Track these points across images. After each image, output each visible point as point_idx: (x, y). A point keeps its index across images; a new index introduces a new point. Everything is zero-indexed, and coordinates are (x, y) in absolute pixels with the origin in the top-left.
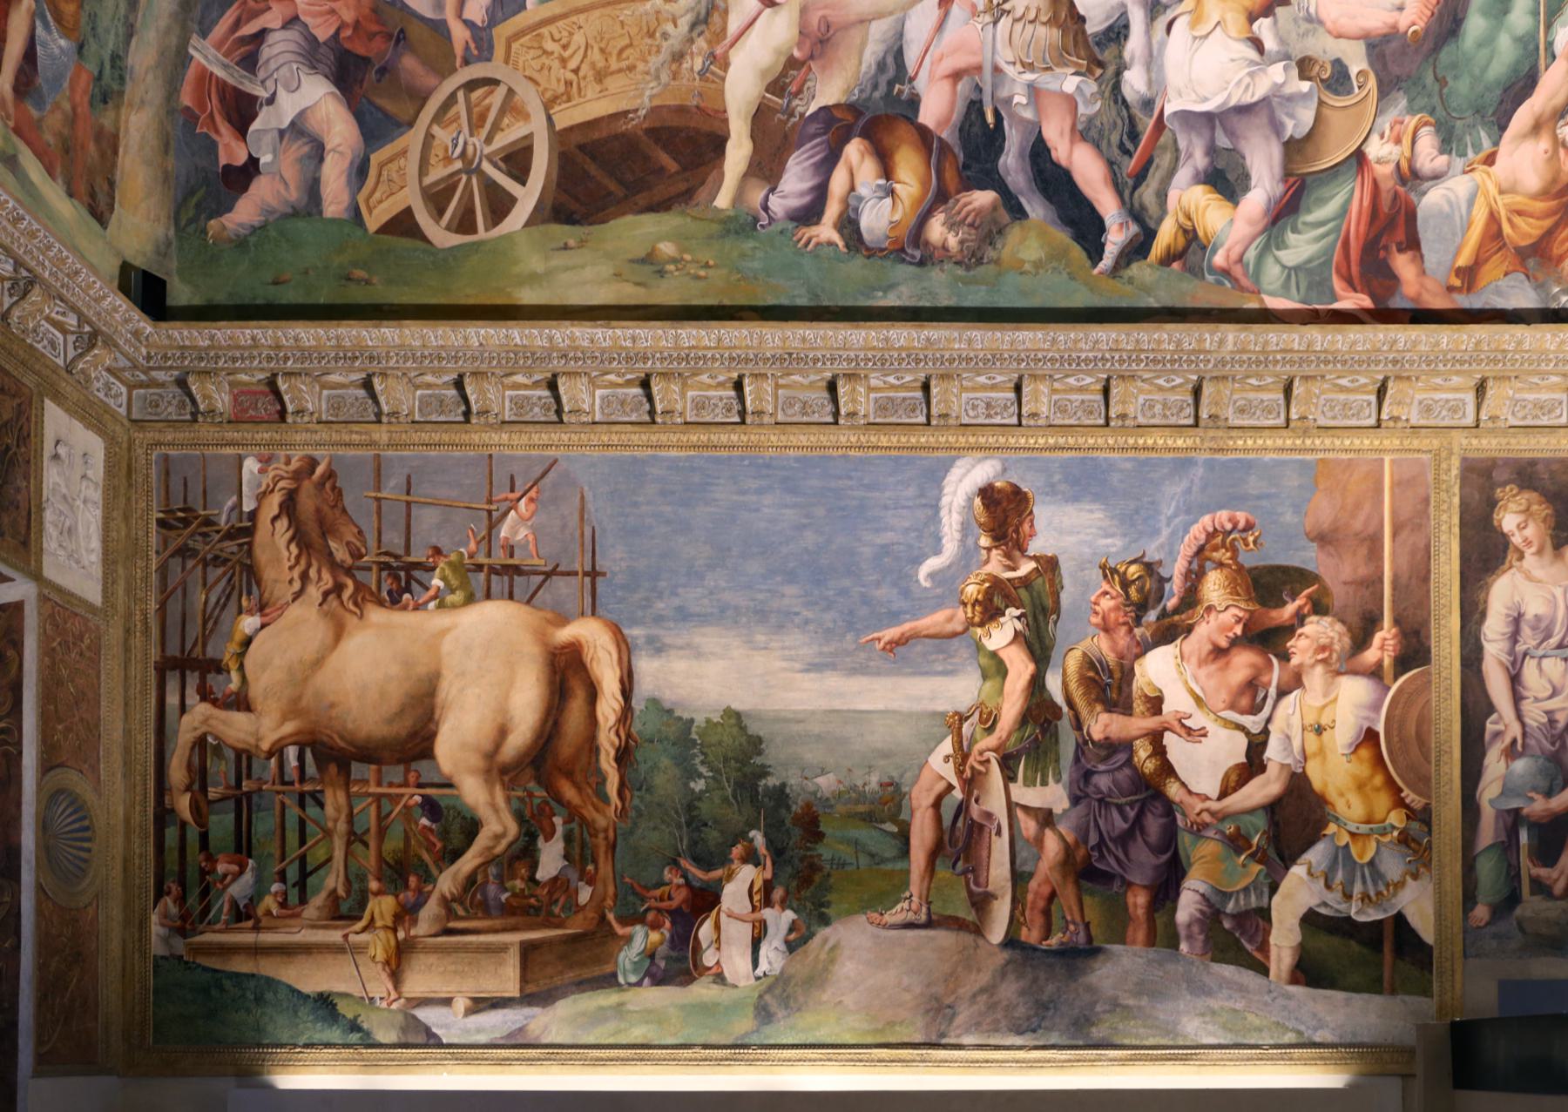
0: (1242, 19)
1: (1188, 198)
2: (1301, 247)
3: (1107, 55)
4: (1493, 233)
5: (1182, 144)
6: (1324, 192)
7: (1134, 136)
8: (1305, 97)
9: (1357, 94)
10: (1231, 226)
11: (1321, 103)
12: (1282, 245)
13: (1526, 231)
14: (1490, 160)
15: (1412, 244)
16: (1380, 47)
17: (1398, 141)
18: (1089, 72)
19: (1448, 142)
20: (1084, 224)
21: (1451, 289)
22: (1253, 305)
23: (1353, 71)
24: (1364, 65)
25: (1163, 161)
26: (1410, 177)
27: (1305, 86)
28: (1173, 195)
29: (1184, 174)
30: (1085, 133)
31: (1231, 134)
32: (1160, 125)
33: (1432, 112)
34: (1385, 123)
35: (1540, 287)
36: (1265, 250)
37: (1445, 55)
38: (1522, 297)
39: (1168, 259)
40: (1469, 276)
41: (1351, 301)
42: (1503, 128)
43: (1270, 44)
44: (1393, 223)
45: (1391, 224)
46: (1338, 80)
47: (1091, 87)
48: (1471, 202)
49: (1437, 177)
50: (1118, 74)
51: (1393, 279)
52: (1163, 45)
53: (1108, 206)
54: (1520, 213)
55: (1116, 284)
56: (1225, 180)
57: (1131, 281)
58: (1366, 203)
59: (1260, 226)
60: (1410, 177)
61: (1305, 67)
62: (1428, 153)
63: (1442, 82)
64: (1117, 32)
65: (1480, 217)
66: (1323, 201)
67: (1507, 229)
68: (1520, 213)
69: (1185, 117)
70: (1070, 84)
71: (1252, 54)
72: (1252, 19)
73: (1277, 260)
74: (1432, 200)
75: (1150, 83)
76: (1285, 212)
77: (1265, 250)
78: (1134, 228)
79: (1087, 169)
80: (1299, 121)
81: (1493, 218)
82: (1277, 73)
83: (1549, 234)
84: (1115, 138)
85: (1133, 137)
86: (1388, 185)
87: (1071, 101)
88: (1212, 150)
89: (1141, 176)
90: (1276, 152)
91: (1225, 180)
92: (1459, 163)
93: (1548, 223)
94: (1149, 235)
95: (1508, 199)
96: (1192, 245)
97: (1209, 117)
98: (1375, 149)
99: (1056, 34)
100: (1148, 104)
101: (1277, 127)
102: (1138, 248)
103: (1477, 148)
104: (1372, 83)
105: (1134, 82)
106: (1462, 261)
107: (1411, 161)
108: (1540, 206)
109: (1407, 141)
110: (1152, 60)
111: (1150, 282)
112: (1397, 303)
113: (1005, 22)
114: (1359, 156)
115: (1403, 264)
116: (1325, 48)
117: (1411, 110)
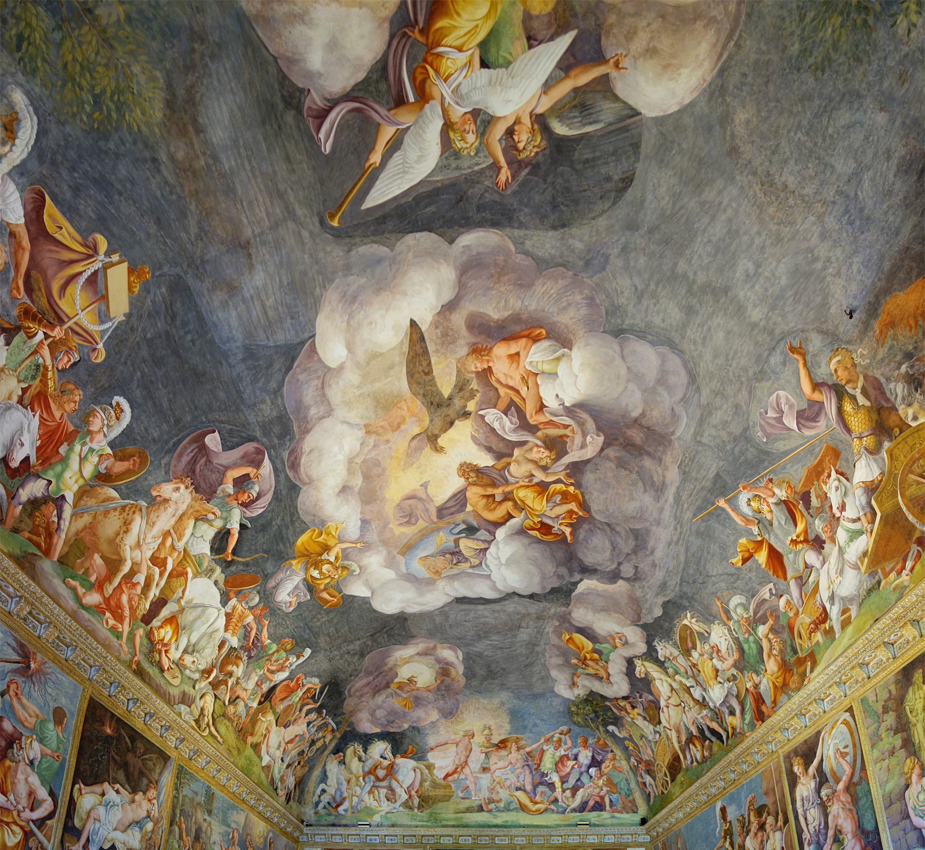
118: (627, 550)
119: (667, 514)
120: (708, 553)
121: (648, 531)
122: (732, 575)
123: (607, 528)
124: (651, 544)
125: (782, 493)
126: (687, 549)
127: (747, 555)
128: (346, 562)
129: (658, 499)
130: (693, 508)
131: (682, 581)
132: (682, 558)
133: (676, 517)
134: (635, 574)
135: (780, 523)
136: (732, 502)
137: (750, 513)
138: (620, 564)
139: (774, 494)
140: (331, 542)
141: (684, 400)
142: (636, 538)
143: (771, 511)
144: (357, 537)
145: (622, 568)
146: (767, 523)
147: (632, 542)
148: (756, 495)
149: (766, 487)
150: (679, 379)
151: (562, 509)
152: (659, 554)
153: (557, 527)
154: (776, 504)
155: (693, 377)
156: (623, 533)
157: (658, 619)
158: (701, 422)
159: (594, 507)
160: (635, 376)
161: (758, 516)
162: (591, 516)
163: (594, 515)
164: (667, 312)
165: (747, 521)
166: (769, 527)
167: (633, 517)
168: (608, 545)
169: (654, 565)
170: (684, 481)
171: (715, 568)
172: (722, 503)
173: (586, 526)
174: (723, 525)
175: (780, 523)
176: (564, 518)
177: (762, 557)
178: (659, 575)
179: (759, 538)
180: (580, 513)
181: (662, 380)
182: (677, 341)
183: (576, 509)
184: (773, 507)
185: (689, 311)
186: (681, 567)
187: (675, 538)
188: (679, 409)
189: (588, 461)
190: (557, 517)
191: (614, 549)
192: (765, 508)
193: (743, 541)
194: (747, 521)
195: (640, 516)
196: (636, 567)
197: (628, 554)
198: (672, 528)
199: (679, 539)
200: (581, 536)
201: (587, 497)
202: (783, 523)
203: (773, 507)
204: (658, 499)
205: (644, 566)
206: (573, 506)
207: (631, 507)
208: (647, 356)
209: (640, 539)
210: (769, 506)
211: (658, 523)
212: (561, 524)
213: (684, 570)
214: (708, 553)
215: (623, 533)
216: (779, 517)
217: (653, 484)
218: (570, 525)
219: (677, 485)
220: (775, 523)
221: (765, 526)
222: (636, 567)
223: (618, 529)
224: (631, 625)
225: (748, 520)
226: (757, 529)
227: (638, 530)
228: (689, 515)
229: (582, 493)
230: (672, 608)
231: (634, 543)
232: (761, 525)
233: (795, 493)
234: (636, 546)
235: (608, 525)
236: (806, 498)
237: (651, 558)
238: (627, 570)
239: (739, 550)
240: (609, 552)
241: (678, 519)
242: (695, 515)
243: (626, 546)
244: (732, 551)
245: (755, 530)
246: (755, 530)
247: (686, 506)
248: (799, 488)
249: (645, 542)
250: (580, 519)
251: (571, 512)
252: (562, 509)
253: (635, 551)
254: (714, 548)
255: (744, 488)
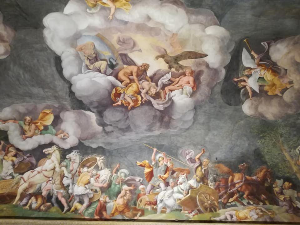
0: (84, 185)
1: (76, 204)
2: (90, 210)
3: (67, 188)
4: (116, 209)
5: (76, 198)
6: (94, 204)
7: (70, 197)
8: (92, 193)
9: (98, 193)
10: (81, 208)
11: (94, 194)
12: (88, 210)
13: (121, 209)
14: (116, 201)
15: (105, 210)
16: (101, 188)
17: (104, 198)
18: (64, 190)
19: (110, 198)
20: (61, 207)
21: (110, 216)
22: (83, 218)
23: (98, 190)
24: (99, 190)
25: (73, 200)
26: (106, 202)
27: (92, 192)
28: (74, 204)
29: (76, 202)
30: (63, 197)
31: (82, 197)
32: (73, 196)
33: (108, 195)
34: (102, 196)
35: (122, 216)
36: (86, 210)
37: (110, 189)
38: (120, 217)
39: (72, 212)
40: (113, 214)
41: (96, 217)
42: (117, 197)
43: (87, 188)
44: (103, 208)
45: (103, 208)
46: (96, 191)
47: (65, 192)
48: (113, 205)
49: (109, 202)
50: (68, 190)
51: (103, 215)
52: (74, 187)
53: (65, 205)
54: (120, 207)
55: (65, 214)
56: (81, 202)
57: (67, 214)
58: (100, 205)
59: (85, 208)
60: (106, 202)
61: (92, 190)
62: (108, 199)
63: (109, 192)
64: (68, 186)
65: (115, 207)
66: (94, 205)
67: (118, 209)
68: (120, 207)
69: (77, 195)
70: (62, 191)
71: (85, 188)
72: (85, 185)
73: (87, 212)
74: (108, 205)
75: (72, 191)
76: (89, 206)
77: (86, 210)
78: (68, 208)
79: (63, 201)
80: (91, 196)
81: (116, 207)
82: (88, 191)
83: (124, 209)
84: (67, 197)
85: (70, 198)
86: (103, 203)
87: (62, 193)
88: (80, 199)
89: (70, 202)
90: (88, 199)
91: (81, 202)
92: (112, 201)
93: (123, 208)
94: (70, 209)
95: (119, 205)
96: (76, 210)
97: (79, 195)
98: (101, 199)
99: (60, 186)
100: (72, 194)
101: (88, 196)
102: (69, 210)
103: (114, 199)
104: (100, 192)
105: (70, 191)
106: (112, 213)
107: (106, 200)
108: (122, 206)
109: (105, 198)
110: (72, 189)
111: (69, 215)
112: (103, 218)
113: (54, 185)
114: (99, 200)
115: (104, 213)
116: (94, 188)
117: (105, 195)
118: (119, 126)
119: (142, 135)
120: (135, 153)
121: (131, 131)
122: (132, 164)
123: (126, 117)
124: (126, 133)
125: (169, 165)
126: (131, 146)
127: (143, 165)
128: (99, 8)
129: (146, 130)
130: (148, 142)
131: (117, 149)
132: (127, 146)
133: (142, 138)
134: (109, 132)
135: (161, 169)
136: (157, 153)
137: (157, 159)
138: (111, 125)
139: (167, 163)
140: (118, 4)
141: (181, 129)
142: (126, 128)
143: (162, 165)
144: (118, 18)
145: (109, 126)
146: (158, 165)
147: (124, 127)
148: (163, 158)
149: (168, 160)
150: (187, 126)
151: (129, 100)
152: (124, 137)
153: (120, 99)
154: (165, 165)
155: (188, 129)
156: (126, 123)
157: (89, 147)
158: (177, 135)
159: (134, 111)
160: (184, 115)
161: (158, 162)
162: (129, 111)
163: (130, 112)
164: (202, 119)
165: (154, 160)
166: (157, 167)
167: (135, 125)
168: (117, 119)
169: (118, 138)
170: (156, 136)
171: (130, 158)
172: (155, 150)
173: (124, 110)
174: (148, 153)
175: (161, 169)
176: (125, 101)
177: (147, 170)
178: (114, 141)
179: (152, 166)
180: (129, 107)
181: (185, 122)
182: (196, 123)
183: (131, 105)
184: (163, 164)
185: (203, 124)
186: (123, 147)
187: (134, 141)
188: (178, 129)
189: (153, 106)
190: (125, 99)
191: (117, 121)
192: (162, 162)
193: (147, 162)
194: (154, 160)
195: (136, 127)
196: (113, 132)
197: (117, 127)
198: (137, 138)
199: (134, 142)
200: (118, 109)
201: (138, 108)
202: (162, 170)
203: (163, 164)
204: (146, 130)
205: (115, 134)
206: (132, 104)
207: (138, 123)
208: (190, 117)
209: (128, 129)
210: (163, 163)
211: (137, 133)
212: (122, 101)
213: (123, 148)
214: (135, 153)
215: (126, 123)
216: (162, 168)
217: (152, 128)
218: (122, 104)
219: (155, 135)
220: (160, 168)
221: (156, 165)
222: (113, 132)
223: (128, 121)
224: (78, 138)
225: (155, 159)
226: (154, 163)
227: (130, 128)
228: (145, 142)
229: (139, 106)
230: (100, 151)
231: (124, 128)
232: (156, 164)
233: (172, 168)
234: (123, 129)
235: (128, 117)
236: (173, 172)
237: (119, 135)
238: (109, 129)
239: (143, 162)
240: (115, 120)
241: (142, 139)
242: (146, 144)
243: (121, 125)
244: (141, 160)
245: (153, 163)
246: (153, 163)
247: (148, 140)
248: (174, 169)
249: (126, 132)
250: (127, 107)
251: (129, 104)
252: (129, 100)
253: (120, 129)
254: (138, 154)
255: (163, 154)
